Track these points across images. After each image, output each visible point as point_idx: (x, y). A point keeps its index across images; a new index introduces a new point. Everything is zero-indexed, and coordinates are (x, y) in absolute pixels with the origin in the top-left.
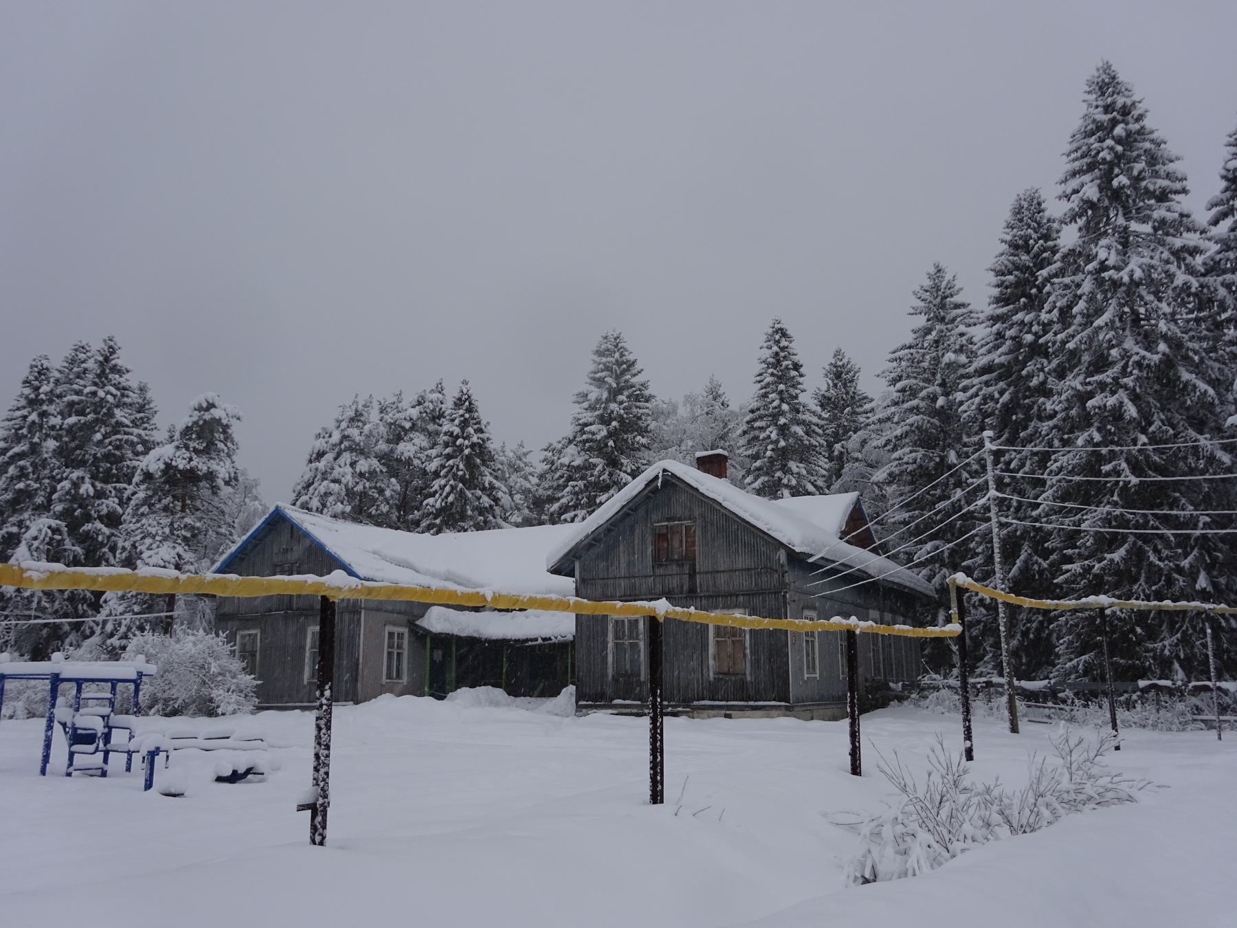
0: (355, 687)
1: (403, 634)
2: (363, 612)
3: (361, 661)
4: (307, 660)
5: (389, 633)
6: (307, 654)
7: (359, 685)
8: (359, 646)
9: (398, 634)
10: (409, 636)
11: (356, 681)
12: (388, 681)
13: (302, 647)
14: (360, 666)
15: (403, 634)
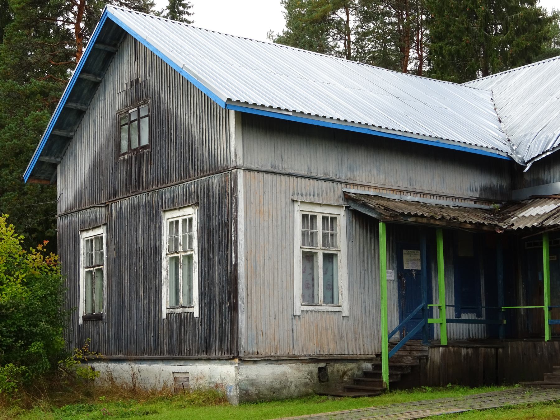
0: (234, 321)
1: (333, 219)
2: (241, 174)
3: (241, 270)
4: (164, 274)
5: (304, 217)
6: (165, 263)
7: (242, 317)
8: (236, 241)
9: (324, 219)
10: (349, 224)
11: (234, 308)
12: (306, 308)
13: (157, 251)
14: (242, 281)
15: (333, 219)
